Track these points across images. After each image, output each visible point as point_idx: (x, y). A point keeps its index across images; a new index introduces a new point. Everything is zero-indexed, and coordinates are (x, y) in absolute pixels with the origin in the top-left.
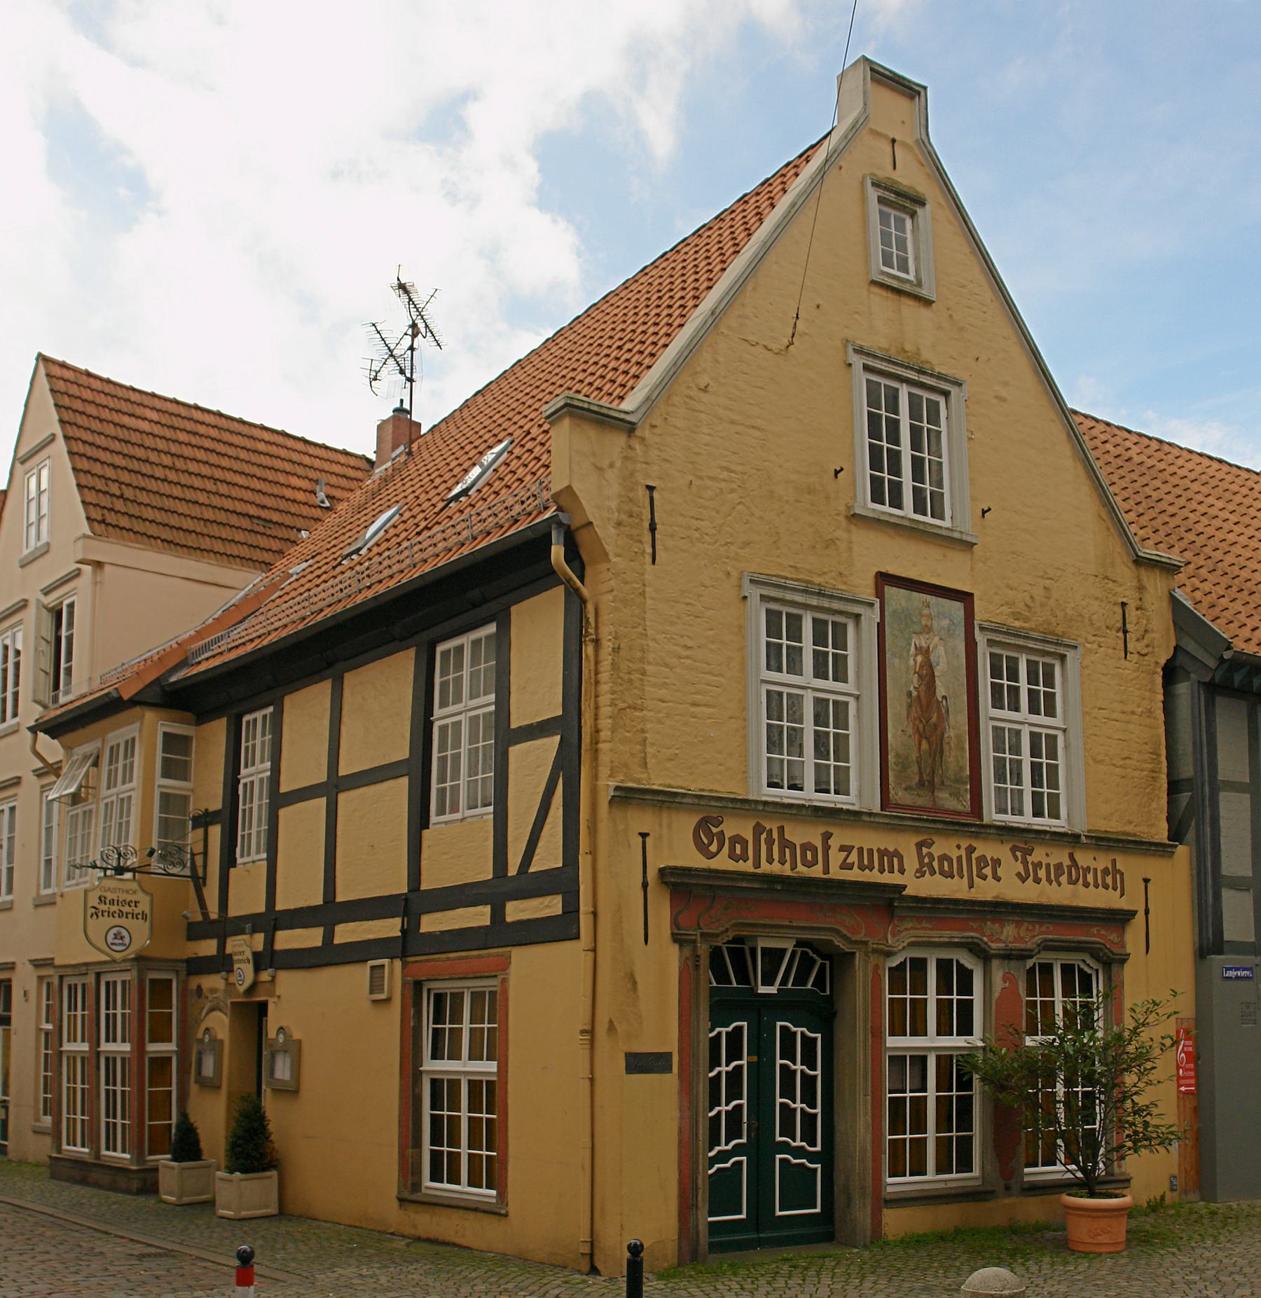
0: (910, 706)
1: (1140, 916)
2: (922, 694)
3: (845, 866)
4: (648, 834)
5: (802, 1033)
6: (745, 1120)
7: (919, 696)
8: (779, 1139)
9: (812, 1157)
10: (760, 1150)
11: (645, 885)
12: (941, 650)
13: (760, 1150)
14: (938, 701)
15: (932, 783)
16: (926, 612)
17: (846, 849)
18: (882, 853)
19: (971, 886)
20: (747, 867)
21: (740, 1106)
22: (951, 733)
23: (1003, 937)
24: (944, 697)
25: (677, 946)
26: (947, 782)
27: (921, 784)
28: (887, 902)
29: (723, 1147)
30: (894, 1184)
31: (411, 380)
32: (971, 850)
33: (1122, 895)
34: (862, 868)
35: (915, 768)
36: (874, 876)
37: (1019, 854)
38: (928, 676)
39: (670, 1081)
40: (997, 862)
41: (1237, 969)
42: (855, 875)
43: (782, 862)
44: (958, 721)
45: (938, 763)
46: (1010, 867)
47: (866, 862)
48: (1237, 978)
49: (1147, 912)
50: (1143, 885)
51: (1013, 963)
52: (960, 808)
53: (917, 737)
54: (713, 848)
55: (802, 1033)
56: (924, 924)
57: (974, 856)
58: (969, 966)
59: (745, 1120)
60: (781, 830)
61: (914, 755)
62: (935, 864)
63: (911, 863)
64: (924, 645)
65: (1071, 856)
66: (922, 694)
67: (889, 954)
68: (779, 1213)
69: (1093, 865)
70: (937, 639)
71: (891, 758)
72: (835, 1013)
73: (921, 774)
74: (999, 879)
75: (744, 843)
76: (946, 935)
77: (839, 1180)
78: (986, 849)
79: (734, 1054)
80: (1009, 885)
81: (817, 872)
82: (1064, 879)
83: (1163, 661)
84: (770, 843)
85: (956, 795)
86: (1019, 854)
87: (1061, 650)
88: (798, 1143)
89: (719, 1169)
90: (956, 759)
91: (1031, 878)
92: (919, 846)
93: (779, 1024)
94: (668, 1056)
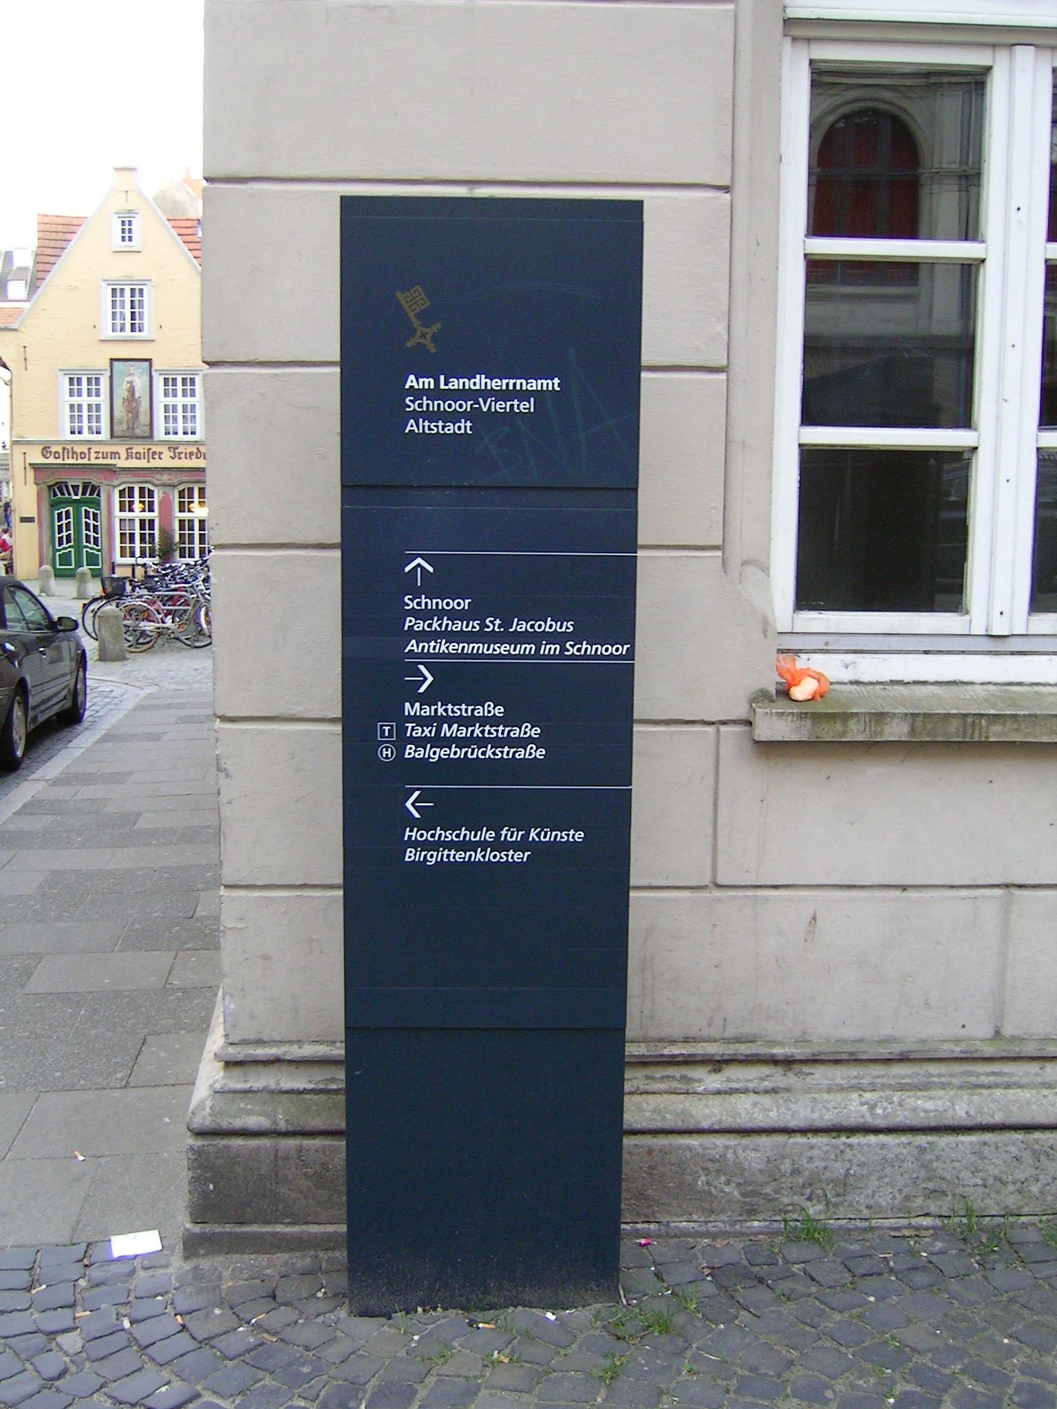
20: (60, 461)
28: (110, 470)
38: (132, 391)
39: (35, 525)
44: (145, 405)
46: (167, 454)
63: (123, 455)
71: (115, 420)
76: (141, 479)
80: (166, 461)
81: (85, 461)
90: (144, 419)
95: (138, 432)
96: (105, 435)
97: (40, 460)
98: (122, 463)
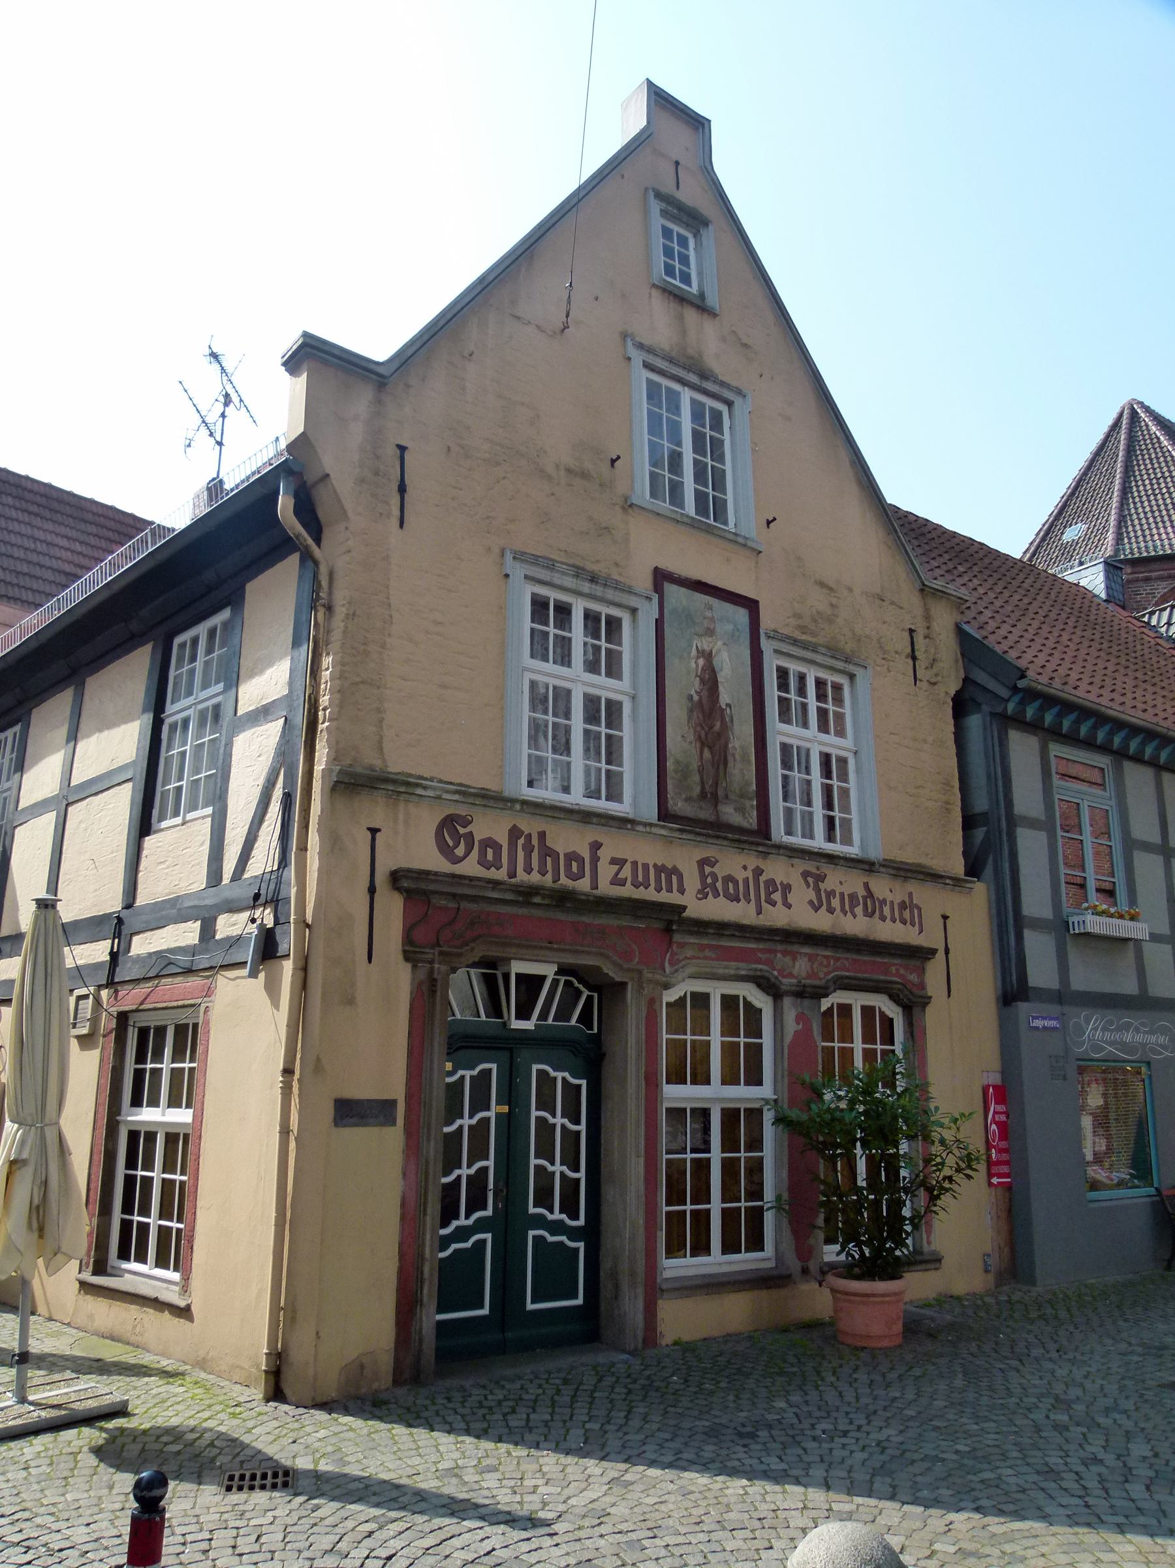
0: (691, 711)
1: (941, 954)
2: (704, 700)
3: (617, 881)
4: (379, 830)
5: (564, 1079)
6: (491, 1186)
7: (700, 701)
8: (532, 1210)
9: (574, 1234)
10: (508, 1226)
11: (372, 890)
12: (725, 655)
13: (508, 1226)
14: (722, 710)
15: (715, 795)
16: (708, 614)
17: (619, 862)
18: (659, 869)
19: (759, 912)
20: (501, 874)
21: (486, 1169)
22: (735, 744)
23: (795, 972)
24: (728, 705)
25: (409, 966)
26: (732, 796)
27: (703, 795)
29: (462, 1222)
30: (676, 1267)
31: (220, 444)
32: (758, 872)
33: (921, 932)
34: (636, 885)
35: (696, 778)
36: (650, 894)
37: (810, 880)
38: (710, 680)
40: (787, 888)
41: (1044, 1018)
42: (628, 891)
43: (543, 873)
45: (721, 774)
46: (801, 895)
47: (640, 879)
48: (1044, 1027)
49: (947, 951)
50: (942, 921)
51: (807, 1002)
52: (745, 824)
53: (698, 745)
54: (460, 851)
55: (564, 1079)
56: (707, 953)
57: (762, 878)
58: (757, 1004)
59: (491, 1186)
60: (542, 835)
61: (695, 765)
62: (719, 885)
63: (692, 882)
64: (706, 648)
65: (866, 885)
66: (704, 700)
67: (667, 986)
68: (530, 1307)
69: (889, 897)
70: (720, 643)
71: (670, 764)
72: (604, 1055)
73: (702, 783)
74: (789, 906)
75: (497, 847)
77: (606, 1265)
78: (777, 870)
79: (479, 1103)
80: (800, 914)
82: (859, 910)
83: (953, 693)
84: (528, 849)
85: (741, 810)
86: (810, 880)
87: (851, 668)
88: (557, 1215)
89: (456, 1251)
90: (742, 772)
91: (824, 907)
92: (702, 863)
93: (535, 1067)
94: (392, 1103)
95: (730, 813)
96: (637, 796)
97: (426, 856)
98: (699, 908)
